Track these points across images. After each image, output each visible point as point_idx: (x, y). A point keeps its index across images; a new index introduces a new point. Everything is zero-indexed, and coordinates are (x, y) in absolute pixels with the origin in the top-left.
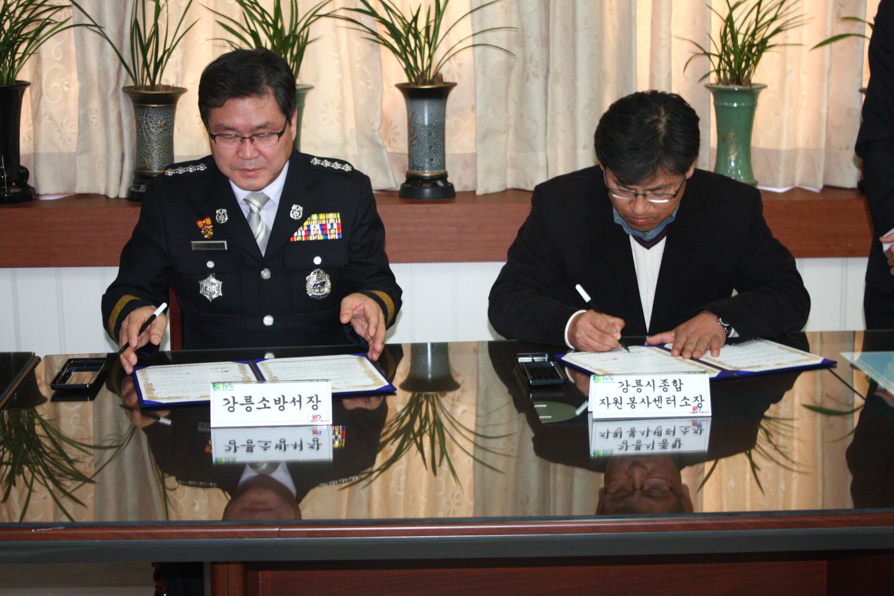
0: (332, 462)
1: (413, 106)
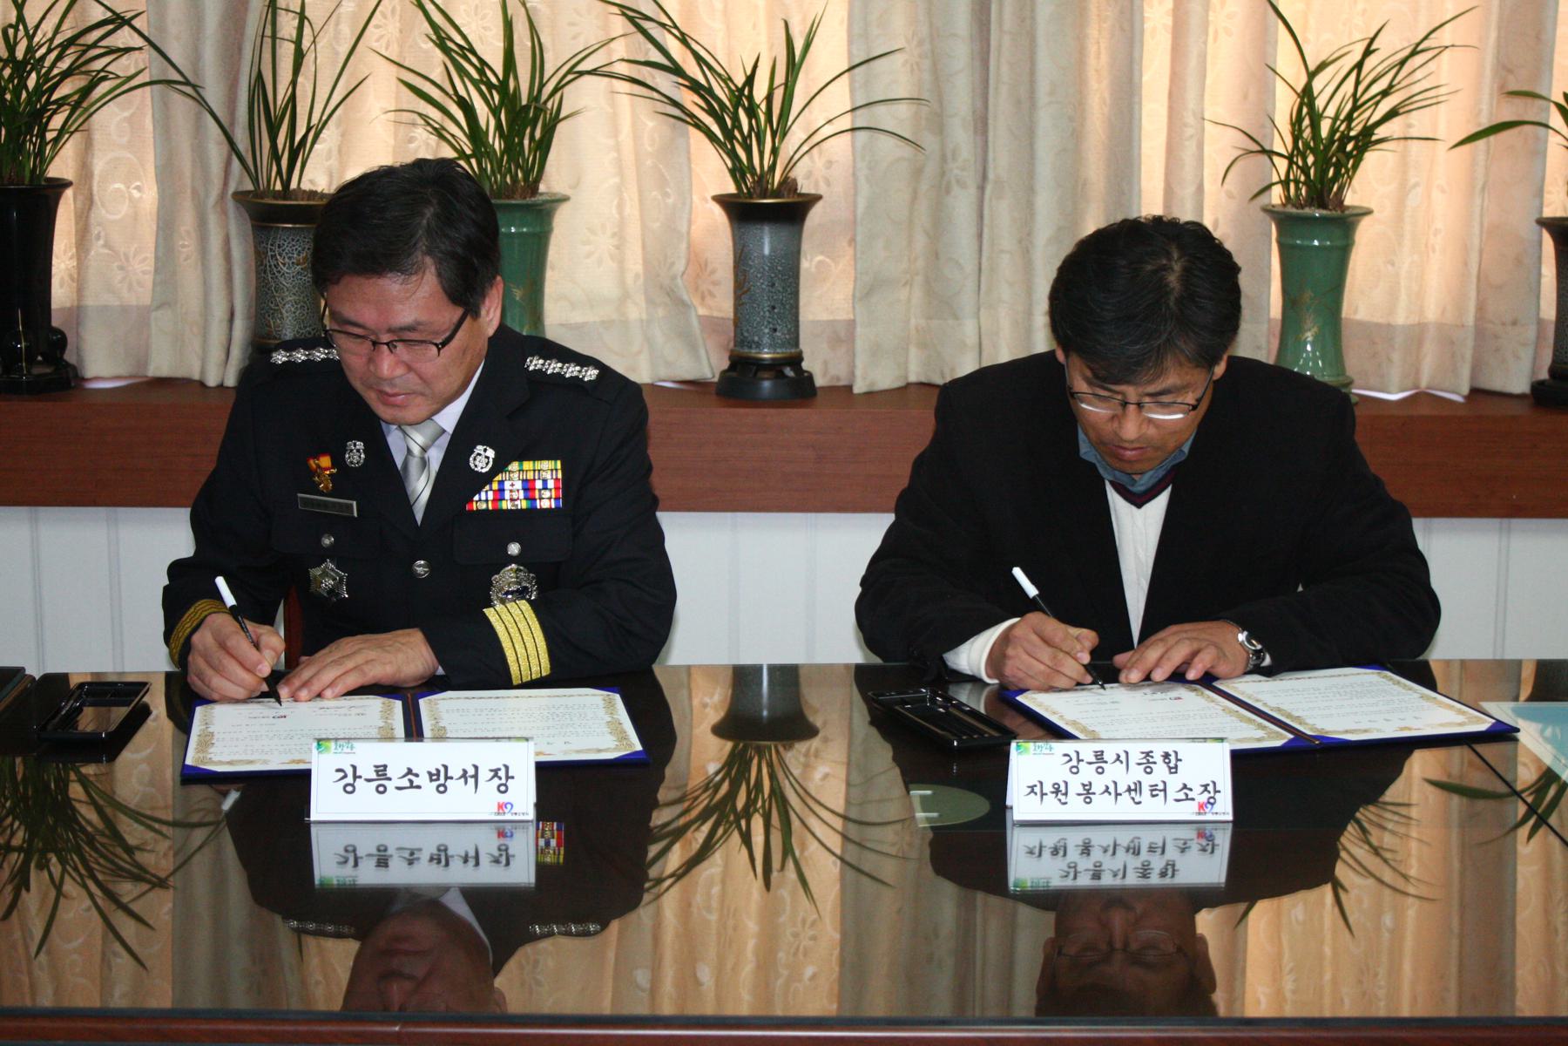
0: (533, 886)
1: (744, 234)
